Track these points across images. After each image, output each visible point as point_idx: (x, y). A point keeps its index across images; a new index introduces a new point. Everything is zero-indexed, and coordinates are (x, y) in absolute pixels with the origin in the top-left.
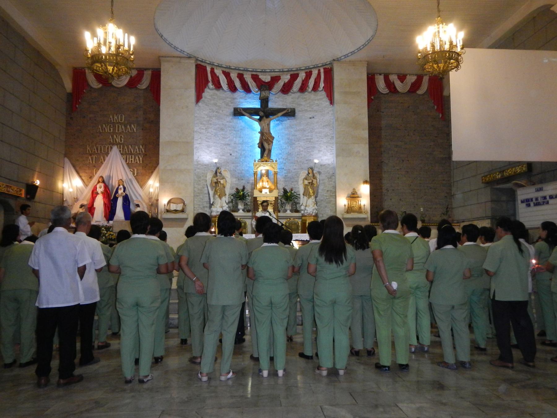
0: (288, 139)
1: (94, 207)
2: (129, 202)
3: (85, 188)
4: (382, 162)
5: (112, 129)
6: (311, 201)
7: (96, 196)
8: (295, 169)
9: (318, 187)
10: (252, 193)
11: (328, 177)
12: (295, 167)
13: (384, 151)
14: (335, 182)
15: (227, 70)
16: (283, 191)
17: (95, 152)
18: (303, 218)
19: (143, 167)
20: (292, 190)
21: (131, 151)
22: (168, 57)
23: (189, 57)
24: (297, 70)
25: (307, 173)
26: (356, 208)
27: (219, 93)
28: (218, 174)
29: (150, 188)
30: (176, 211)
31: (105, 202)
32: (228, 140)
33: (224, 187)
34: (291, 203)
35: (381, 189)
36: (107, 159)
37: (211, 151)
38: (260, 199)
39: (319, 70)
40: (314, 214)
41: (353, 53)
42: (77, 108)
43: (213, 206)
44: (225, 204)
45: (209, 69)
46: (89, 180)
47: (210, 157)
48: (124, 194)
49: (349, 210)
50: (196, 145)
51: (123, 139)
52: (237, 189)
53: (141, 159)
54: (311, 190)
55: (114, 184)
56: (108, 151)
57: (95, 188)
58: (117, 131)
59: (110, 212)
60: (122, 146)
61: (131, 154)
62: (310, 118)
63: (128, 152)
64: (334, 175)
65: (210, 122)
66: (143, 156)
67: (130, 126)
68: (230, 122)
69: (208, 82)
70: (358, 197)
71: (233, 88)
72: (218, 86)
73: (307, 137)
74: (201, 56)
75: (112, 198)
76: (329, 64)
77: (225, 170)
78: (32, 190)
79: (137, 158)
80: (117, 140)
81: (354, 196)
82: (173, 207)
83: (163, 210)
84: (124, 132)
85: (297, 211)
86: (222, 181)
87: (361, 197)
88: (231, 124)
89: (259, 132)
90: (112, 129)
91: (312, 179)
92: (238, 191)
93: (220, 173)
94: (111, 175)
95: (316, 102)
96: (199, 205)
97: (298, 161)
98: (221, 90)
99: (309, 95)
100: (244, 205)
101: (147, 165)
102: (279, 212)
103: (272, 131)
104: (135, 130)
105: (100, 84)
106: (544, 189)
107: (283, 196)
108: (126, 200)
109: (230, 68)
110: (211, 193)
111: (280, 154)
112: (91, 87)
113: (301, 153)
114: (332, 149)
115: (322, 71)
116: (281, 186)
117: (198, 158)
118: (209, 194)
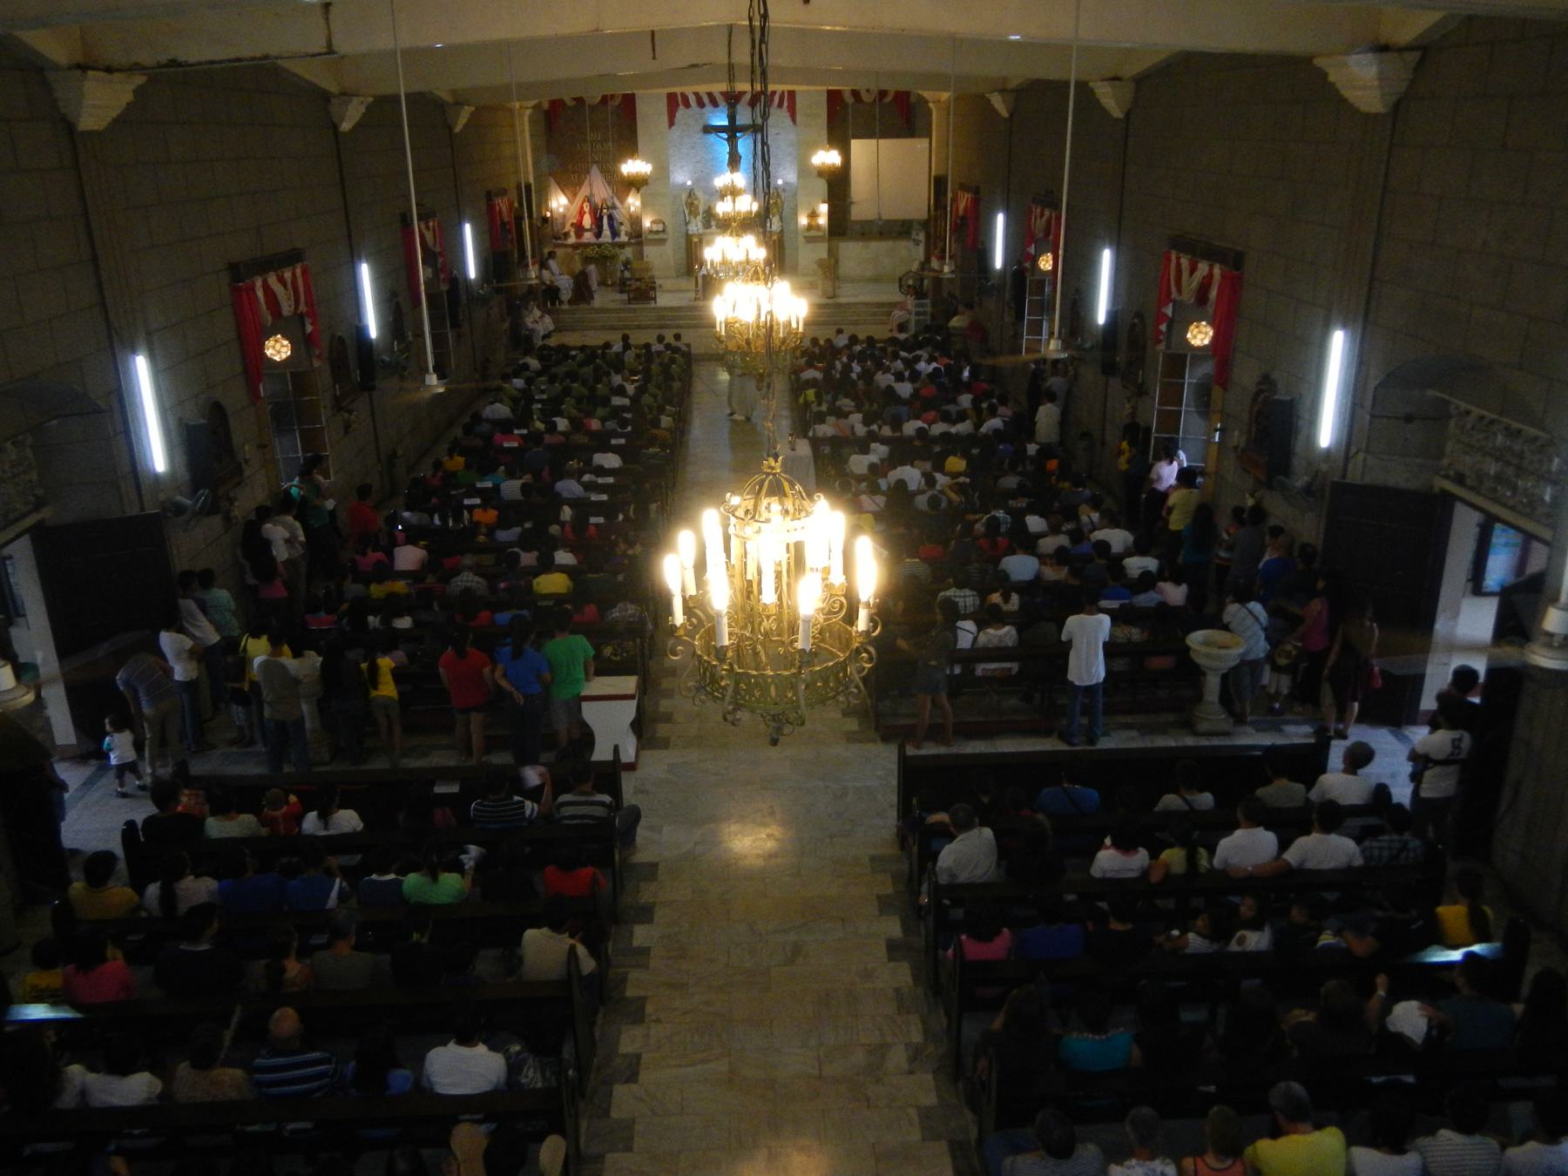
9: (783, 203)
27: (689, 111)
30: (657, 232)
33: (698, 208)
49: (810, 227)
57: (582, 208)
64: (796, 194)
68: (700, 139)
69: (679, 105)
71: (701, 104)
72: (687, 104)
78: (545, 220)
81: (813, 215)
82: (655, 228)
86: (696, 202)
108: (610, 218)
110: (687, 212)
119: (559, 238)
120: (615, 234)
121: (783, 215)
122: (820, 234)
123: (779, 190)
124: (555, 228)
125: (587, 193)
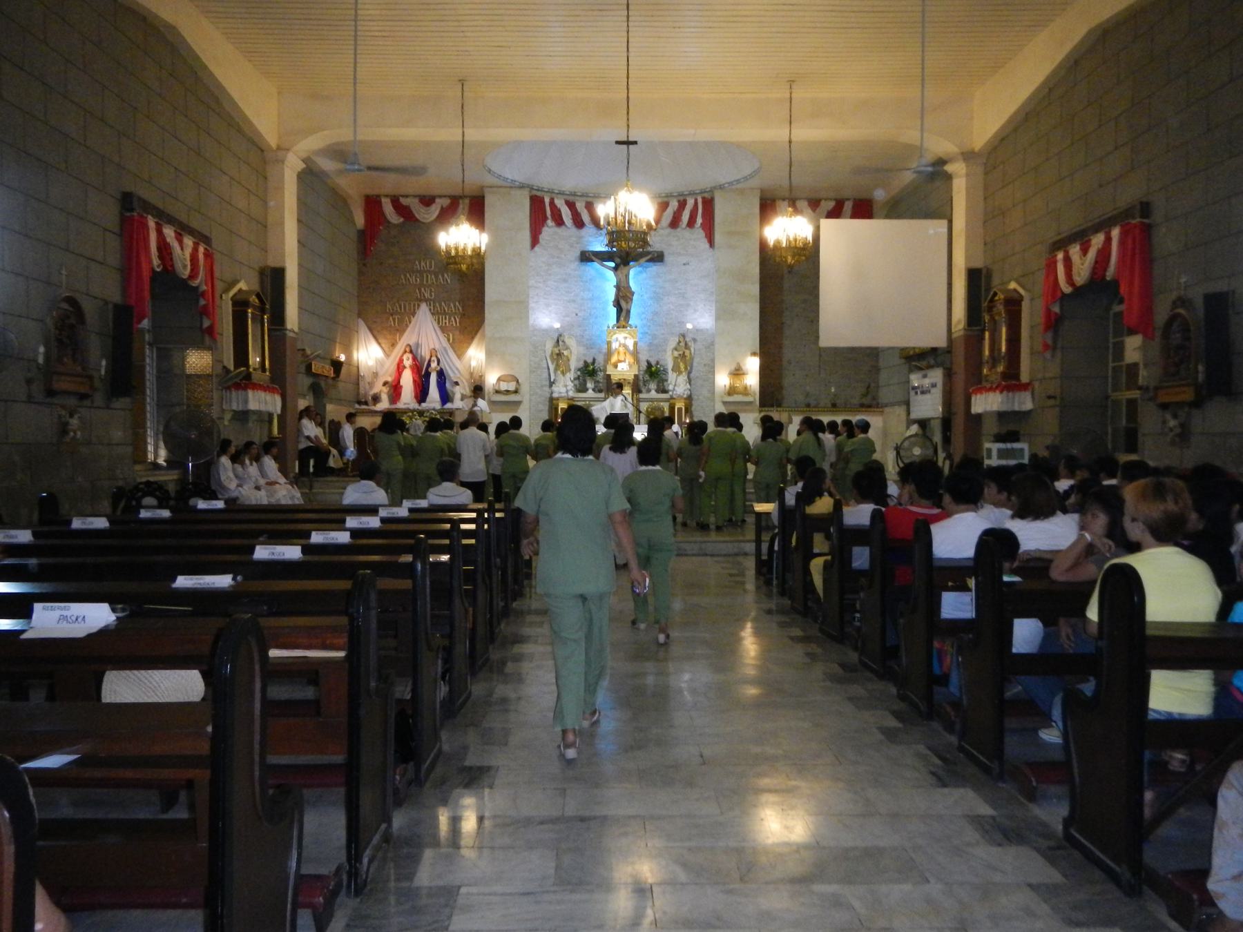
0: (655, 292)
1: (401, 384)
2: (445, 379)
3: (385, 358)
4: (783, 323)
5: (418, 280)
6: (682, 379)
7: (403, 371)
8: (663, 334)
9: (692, 359)
10: (605, 370)
11: (706, 348)
12: (663, 331)
13: (787, 309)
14: (714, 354)
15: (571, 199)
16: (646, 364)
17: (397, 311)
18: (672, 401)
19: (460, 332)
20: (658, 363)
21: (445, 311)
22: (494, 187)
23: (522, 186)
24: (667, 196)
25: (678, 341)
26: (741, 389)
27: (561, 231)
28: (560, 342)
29: (470, 360)
30: (508, 392)
31: (416, 379)
32: (572, 294)
33: (569, 360)
34: (656, 381)
35: (781, 360)
36: (414, 320)
37: (550, 312)
38: (615, 379)
39: (696, 201)
40: (685, 396)
41: (738, 181)
42: (371, 251)
43: (554, 385)
44: (570, 383)
45: (547, 200)
46: (391, 348)
47: (549, 320)
48: (439, 368)
49: (732, 391)
50: (532, 305)
51: (433, 294)
52: (585, 362)
53: (458, 320)
54: (681, 364)
55: (423, 354)
56: (414, 310)
57: (401, 361)
58: (425, 282)
59: (421, 391)
60: (432, 303)
61: (445, 313)
62: (684, 264)
63: (441, 310)
64: (712, 344)
65: (549, 272)
66: (461, 317)
67: (443, 276)
69: (545, 218)
70: (744, 374)
71: (579, 224)
72: (559, 222)
73: (680, 291)
74: (537, 182)
75: (423, 373)
76: (710, 191)
77: (569, 338)
78: (337, 365)
79: (453, 319)
80: (426, 295)
81: (738, 372)
83: (491, 390)
84: (435, 283)
85: (665, 391)
86: (565, 353)
87: (747, 374)
88: (576, 272)
89: (615, 286)
90: (418, 280)
91: (683, 349)
92: (586, 363)
93: (563, 341)
94: (420, 342)
95: (692, 242)
96: (536, 383)
97: (668, 322)
98: (563, 227)
99: (683, 232)
100: (595, 383)
101: (466, 328)
102: (640, 391)
103: (632, 284)
104: (449, 281)
105: (399, 219)
106: (929, 375)
107: (646, 372)
109: (574, 194)
111: (643, 313)
112: (389, 222)
113: (672, 312)
114: (711, 308)
115: (700, 201)
116: (644, 357)
117: (534, 321)
118: (549, 369)
119: (366, 403)
120: (445, 397)
121: (692, 375)
122: (749, 399)
123: (687, 339)
124: (362, 391)
125: (412, 342)
